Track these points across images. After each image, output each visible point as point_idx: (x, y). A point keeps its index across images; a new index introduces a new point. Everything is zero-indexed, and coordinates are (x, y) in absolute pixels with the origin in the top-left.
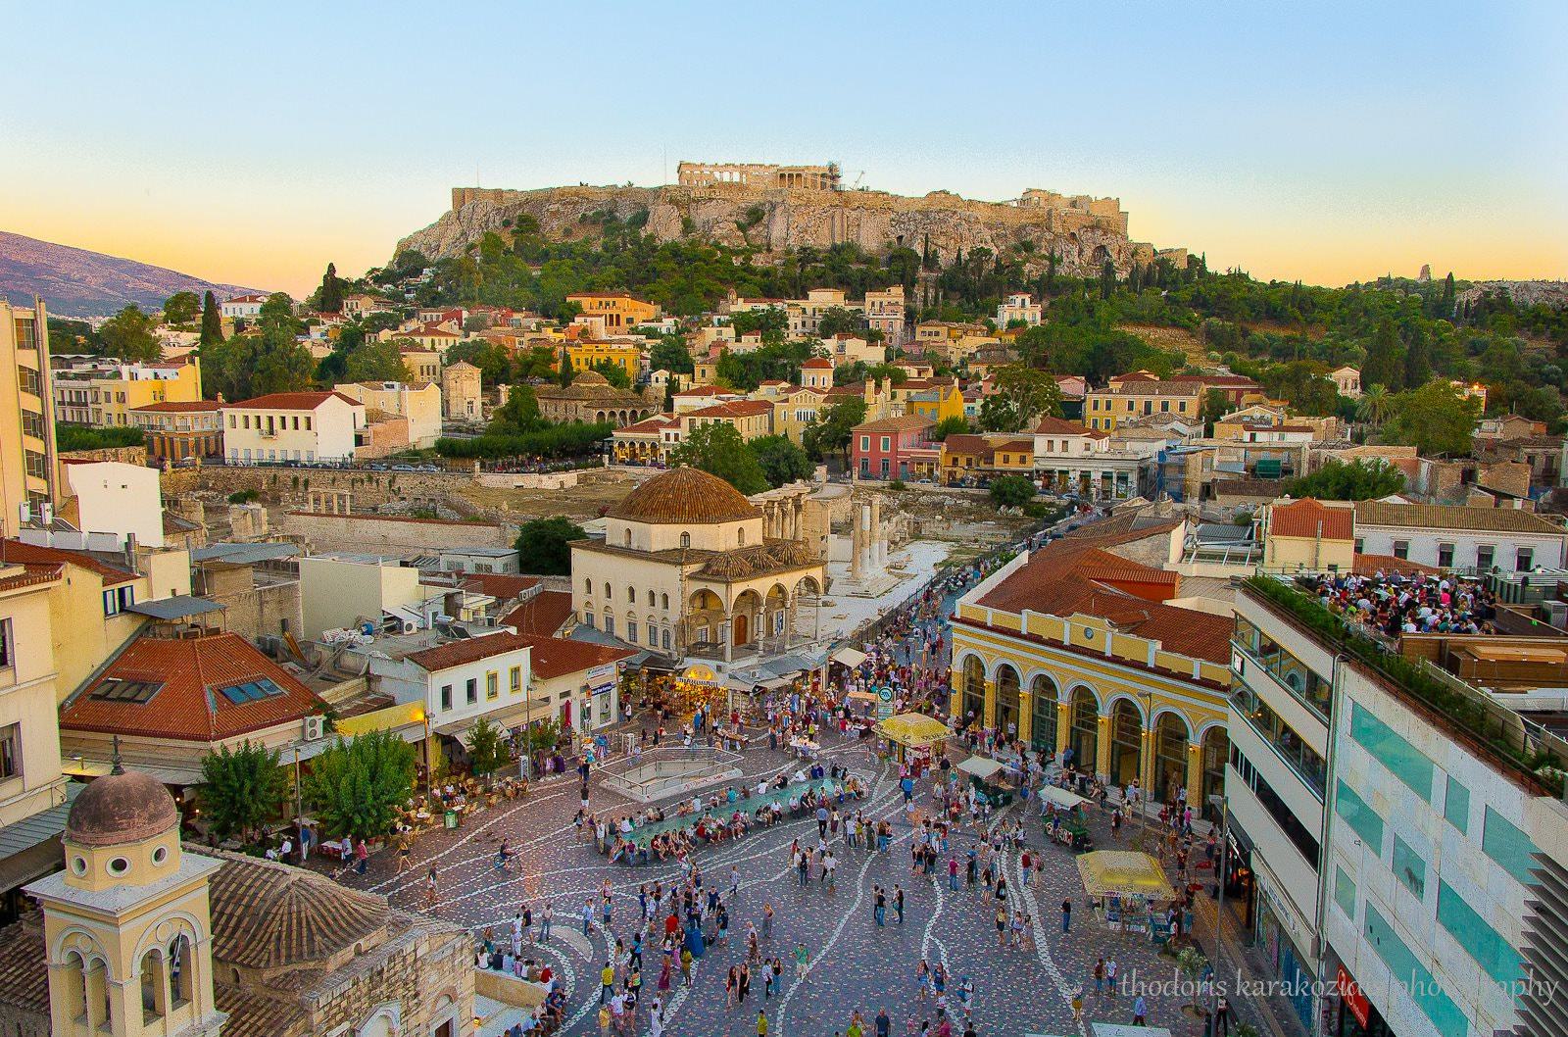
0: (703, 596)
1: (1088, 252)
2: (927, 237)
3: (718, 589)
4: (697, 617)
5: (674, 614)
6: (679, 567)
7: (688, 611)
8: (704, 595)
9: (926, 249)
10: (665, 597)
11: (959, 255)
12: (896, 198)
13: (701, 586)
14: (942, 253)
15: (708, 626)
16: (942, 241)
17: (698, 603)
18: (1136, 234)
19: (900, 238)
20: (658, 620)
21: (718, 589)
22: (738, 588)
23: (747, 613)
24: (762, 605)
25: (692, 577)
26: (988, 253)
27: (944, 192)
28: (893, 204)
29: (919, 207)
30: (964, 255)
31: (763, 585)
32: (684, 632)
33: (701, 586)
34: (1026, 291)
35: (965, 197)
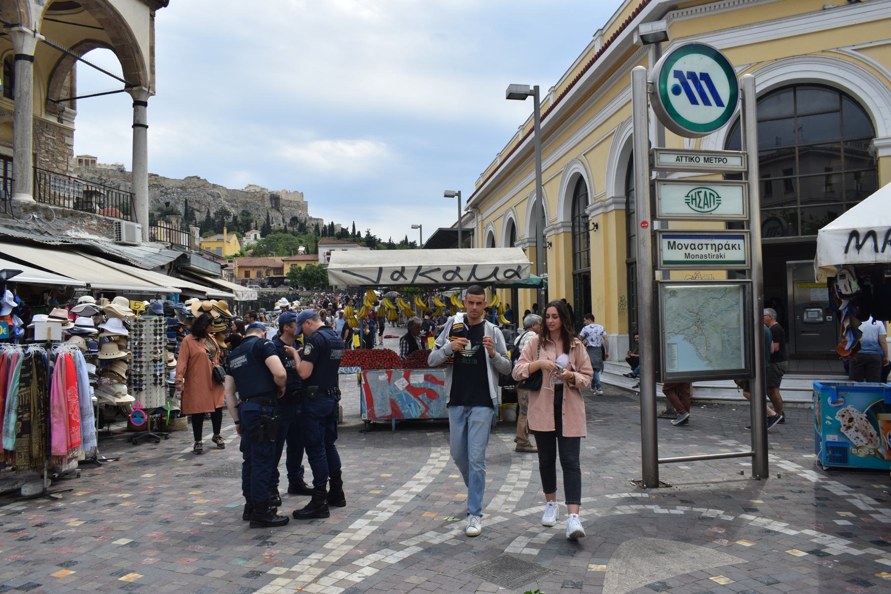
1: (288, 221)
2: (186, 202)
9: (186, 210)
11: (209, 213)
12: (165, 178)
14: (197, 213)
16: (196, 206)
18: (313, 212)
19: (167, 204)
26: (228, 214)
27: (196, 177)
28: (162, 183)
29: (180, 185)
30: (212, 215)
34: (256, 228)
35: (211, 182)
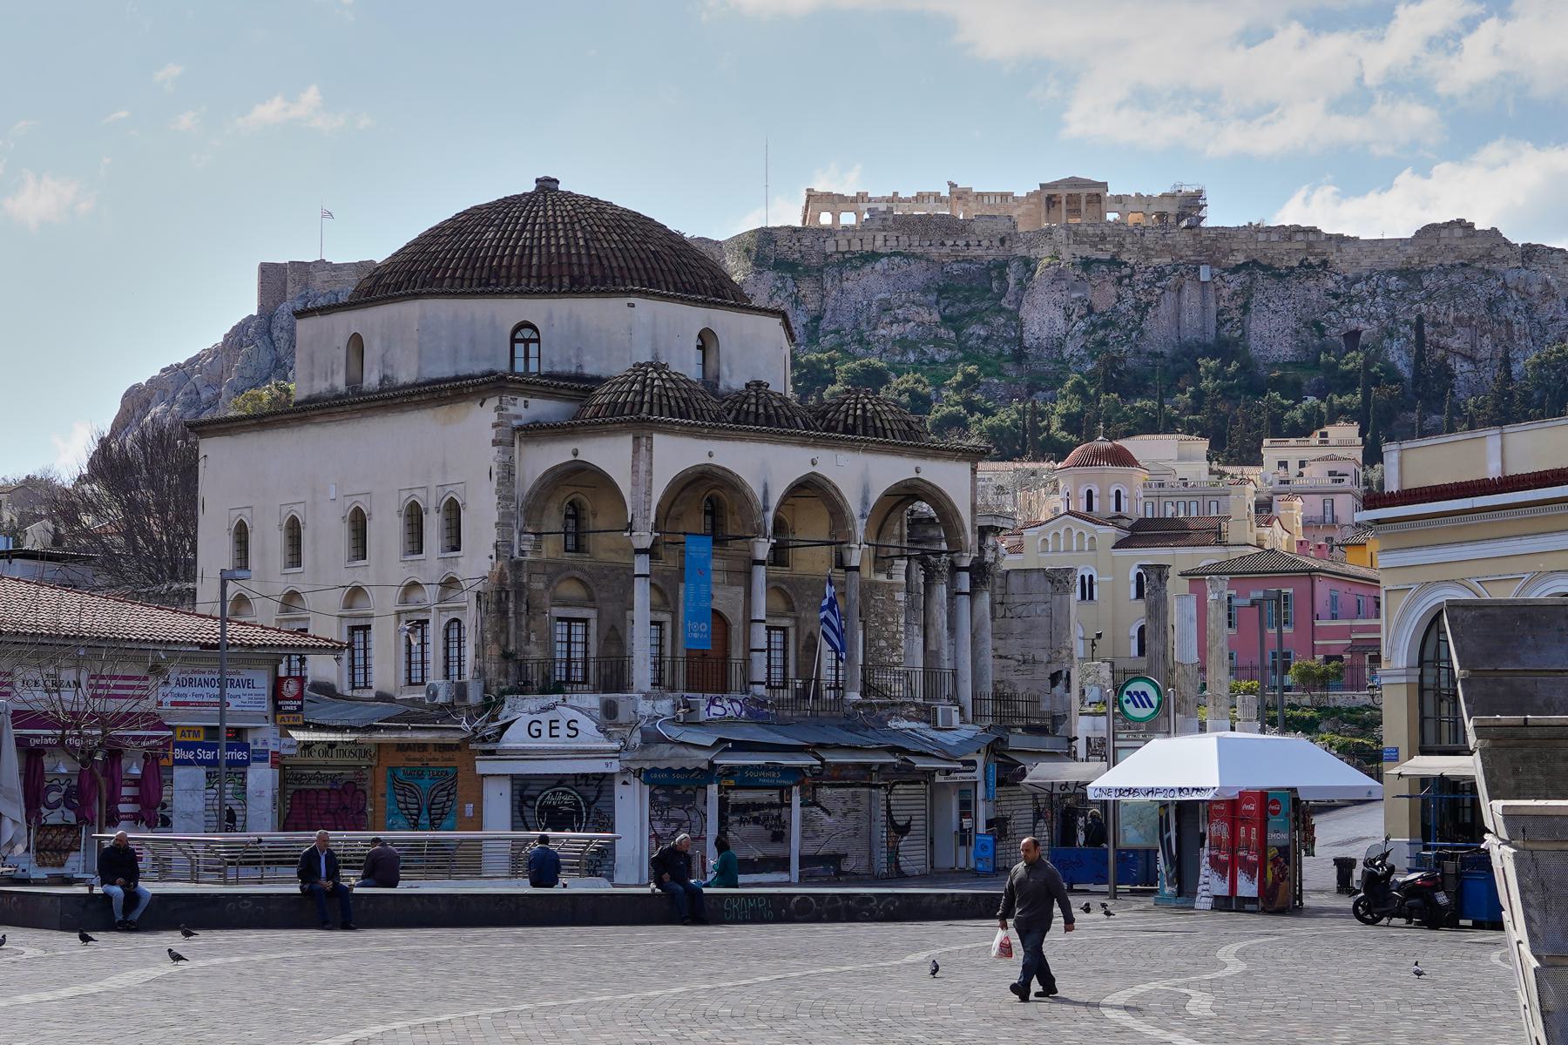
0: (575, 513)
3: (610, 454)
4: (556, 572)
5: (477, 562)
6: (492, 403)
7: (523, 545)
8: (580, 474)
10: (453, 511)
13: (556, 454)
15: (590, 613)
17: (553, 521)
20: (431, 594)
21: (610, 454)
22: (676, 454)
23: (727, 599)
24: (759, 532)
25: (534, 432)
31: (766, 467)
32: (503, 613)
33: (556, 454)
